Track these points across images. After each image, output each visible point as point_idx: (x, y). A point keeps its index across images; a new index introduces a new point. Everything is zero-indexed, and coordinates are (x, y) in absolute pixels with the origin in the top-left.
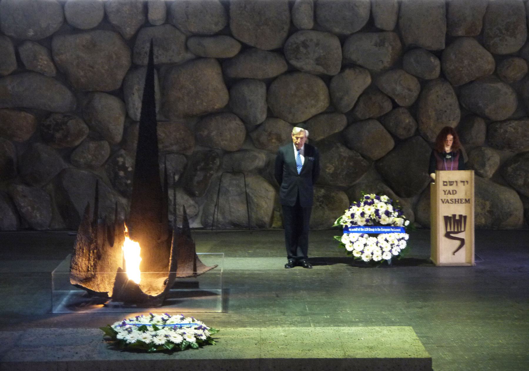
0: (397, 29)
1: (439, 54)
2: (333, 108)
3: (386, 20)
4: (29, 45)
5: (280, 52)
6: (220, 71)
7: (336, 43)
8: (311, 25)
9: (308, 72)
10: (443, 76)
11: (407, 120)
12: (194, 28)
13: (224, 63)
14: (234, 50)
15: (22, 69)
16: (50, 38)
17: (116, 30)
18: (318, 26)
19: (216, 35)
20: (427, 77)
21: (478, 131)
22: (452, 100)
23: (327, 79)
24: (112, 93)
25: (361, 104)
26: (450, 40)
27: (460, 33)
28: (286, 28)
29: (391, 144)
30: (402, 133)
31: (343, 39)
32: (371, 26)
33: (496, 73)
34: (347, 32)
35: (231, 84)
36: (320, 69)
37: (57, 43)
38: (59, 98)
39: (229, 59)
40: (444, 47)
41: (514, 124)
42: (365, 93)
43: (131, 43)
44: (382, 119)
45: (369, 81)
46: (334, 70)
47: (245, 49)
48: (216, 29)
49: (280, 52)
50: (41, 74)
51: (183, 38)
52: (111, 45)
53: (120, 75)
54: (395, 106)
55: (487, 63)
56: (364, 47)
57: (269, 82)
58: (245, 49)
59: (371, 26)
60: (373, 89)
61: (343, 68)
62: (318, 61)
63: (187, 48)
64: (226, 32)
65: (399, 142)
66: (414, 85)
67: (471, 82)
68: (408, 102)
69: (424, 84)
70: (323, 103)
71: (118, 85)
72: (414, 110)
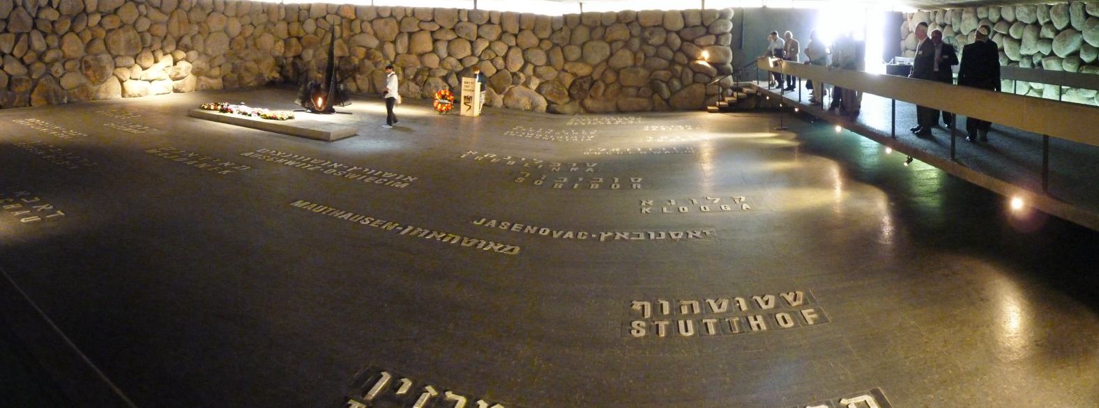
0: (501, 24)
1: (516, 36)
2: (473, 54)
3: (495, 20)
4: (365, 23)
5: (453, 29)
6: (430, 35)
7: (475, 27)
8: (466, 19)
9: (466, 39)
10: (517, 45)
11: (500, 62)
12: (422, 19)
13: (432, 33)
14: (437, 27)
15: (362, 32)
16: (373, 20)
17: (395, 18)
18: (470, 20)
19: (429, 22)
20: (510, 45)
21: (530, 69)
22: (520, 55)
23: (471, 42)
24: (392, 42)
25: (482, 55)
26: (521, 30)
27: (523, 27)
28: (457, 20)
29: (495, 71)
30: (499, 67)
31: (479, 26)
32: (489, 22)
33: (539, 46)
34: (480, 24)
35: (435, 41)
36: (467, 38)
37: (374, 22)
38: (374, 43)
39: (434, 31)
40: (517, 32)
41: (544, 67)
42: (486, 48)
43: (399, 23)
44: (492, 61)
45: (487, 44)
46: (474, 39)
47: (441, 27)
48: (430, 19)
49: (453, 29)
50: (368, 33)
51: (418, 22)
52: (393, 23)
53: (394, 36)
54: (497, 56)
55: (534, 41)
56: (486, 29)
57: (449, 42)
58: (441, 27)
59: (489, 22)
60: (489, 48)
61: (477, 38)
62: (467, 35)
63: (419, 26)
64: (433, 20)
65: (498, 71)
66: (505, 48)
67: (528, 49)
68: (503, 54)
69: (510, 48)
70: (468, 52)
71: (394, 39)
72: (505, 58)
